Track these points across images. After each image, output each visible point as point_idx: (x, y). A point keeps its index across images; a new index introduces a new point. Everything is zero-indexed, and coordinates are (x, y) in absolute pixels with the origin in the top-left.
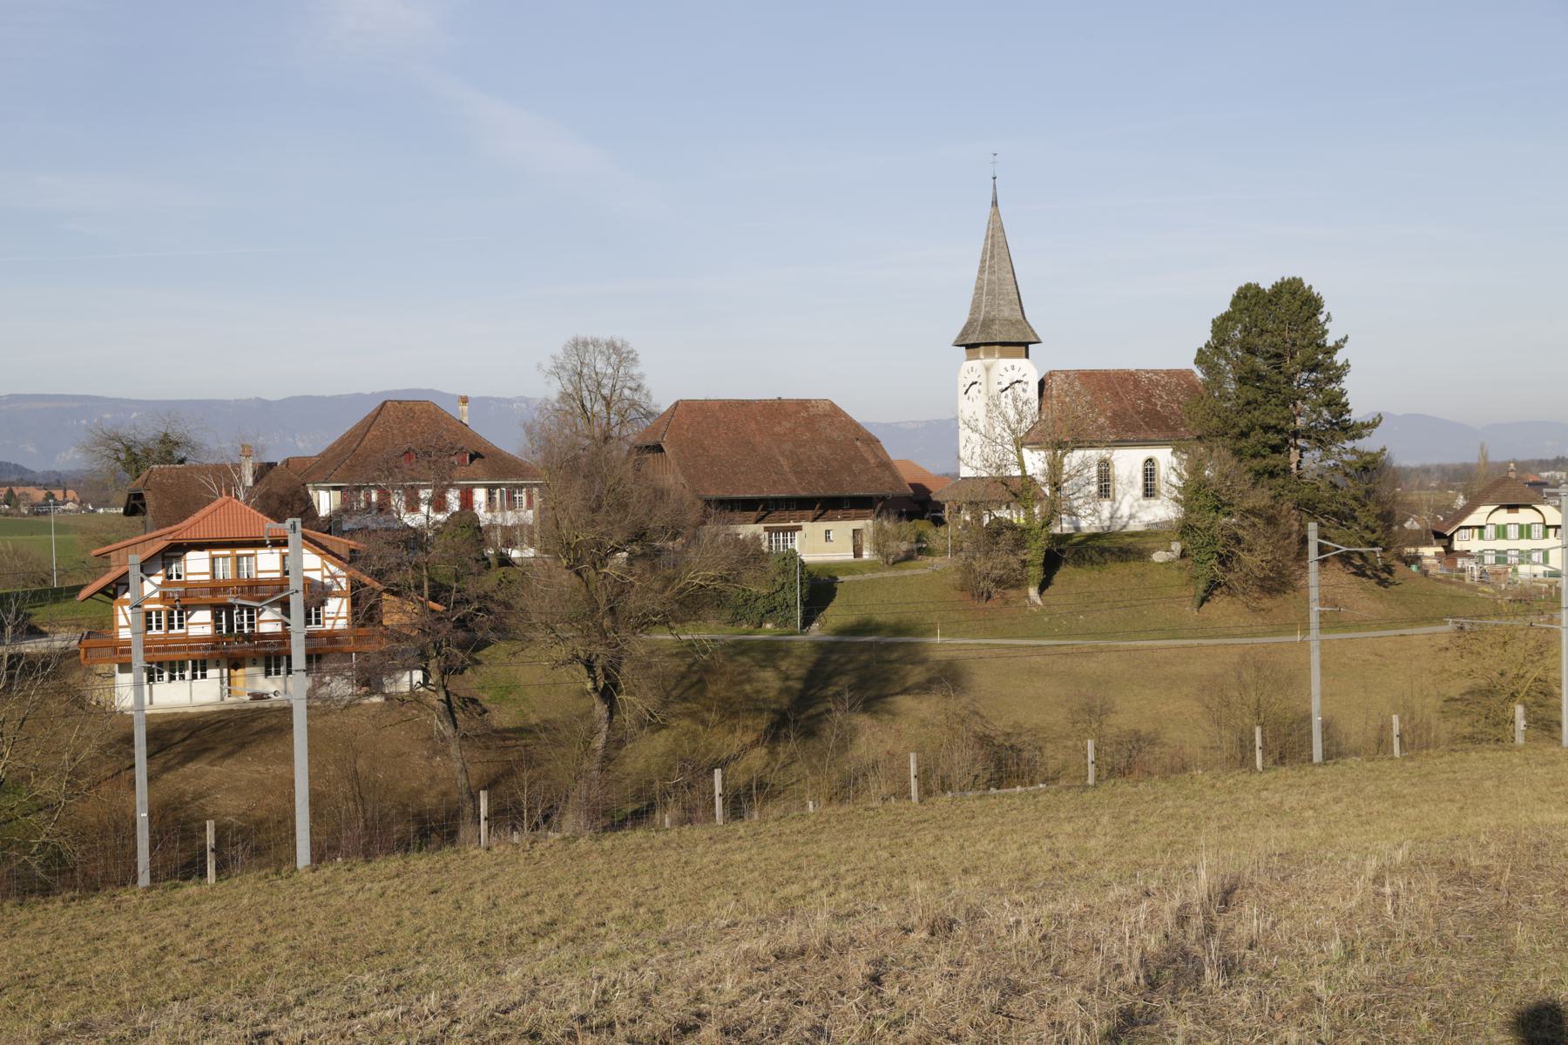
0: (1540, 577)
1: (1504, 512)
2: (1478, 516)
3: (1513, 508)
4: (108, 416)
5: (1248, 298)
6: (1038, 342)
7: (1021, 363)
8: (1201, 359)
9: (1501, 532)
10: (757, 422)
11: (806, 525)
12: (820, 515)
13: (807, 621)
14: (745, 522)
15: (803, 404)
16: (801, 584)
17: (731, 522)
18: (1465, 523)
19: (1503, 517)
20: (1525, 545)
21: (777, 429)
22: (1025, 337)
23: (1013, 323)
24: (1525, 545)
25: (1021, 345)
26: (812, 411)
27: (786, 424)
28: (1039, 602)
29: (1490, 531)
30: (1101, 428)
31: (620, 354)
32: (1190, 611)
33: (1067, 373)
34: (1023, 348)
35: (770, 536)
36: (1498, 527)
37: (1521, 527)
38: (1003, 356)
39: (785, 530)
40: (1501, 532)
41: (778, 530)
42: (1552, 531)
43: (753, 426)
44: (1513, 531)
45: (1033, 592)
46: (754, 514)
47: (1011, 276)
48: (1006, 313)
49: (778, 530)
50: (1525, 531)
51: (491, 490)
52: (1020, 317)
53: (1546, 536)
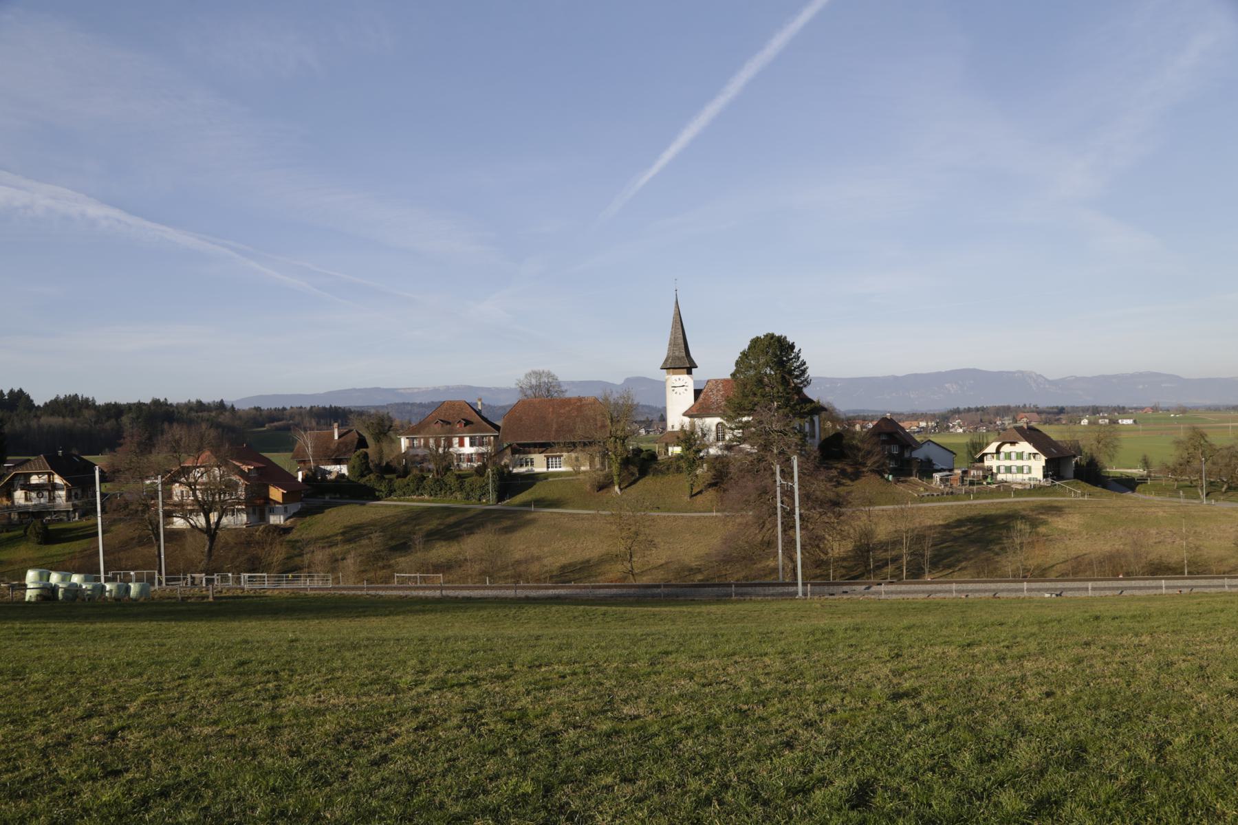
0: (1027, 481)
1: (1008, 445)
2: (992, 448)
3: (1013, 443)
4: (828, 386)
5: (755, 342)
6: (696, 367)
7: (684, 378)
8: (733, 375)
9: (1008, 456)
10: (553, 408)
11: (565, 454)
12: (572, 450)
13: (500, 498)
14: (535, 453)
15: (580, 399)
16: (493, 481)
17: (530, 453)
18: (985, 451)
19: (1006, 448)
20: (1020, 463)
21: (562, 411)
22: (684, 363)
23: (679, 358)
24: (1020, 463)
25: (689, 368)
26: (584, 402)
27: (567, 409)
28: (619, 493)
29: (1002, 455)
30: (719, 407)
31: (549, 375)
32: (686, 498)
33: (716, 381)
34: (685, 370)
35: (548, 459)
36: (1005, 453)
37: (1017, 453)
38: (674, 374)
39: (556, 457)
40: (1008, 456)
41: (552, 457)
42: (1032, 456)
43: (551, 410)
44: (1013, 455)
45: (617, 488)
46: (541, 450)
47: (681, 336)
48: (677, 354)
49: (552, 457)
50: (1020, 456)
51: (471, 438)
52: (684, 354)
53: (1030, 458)
